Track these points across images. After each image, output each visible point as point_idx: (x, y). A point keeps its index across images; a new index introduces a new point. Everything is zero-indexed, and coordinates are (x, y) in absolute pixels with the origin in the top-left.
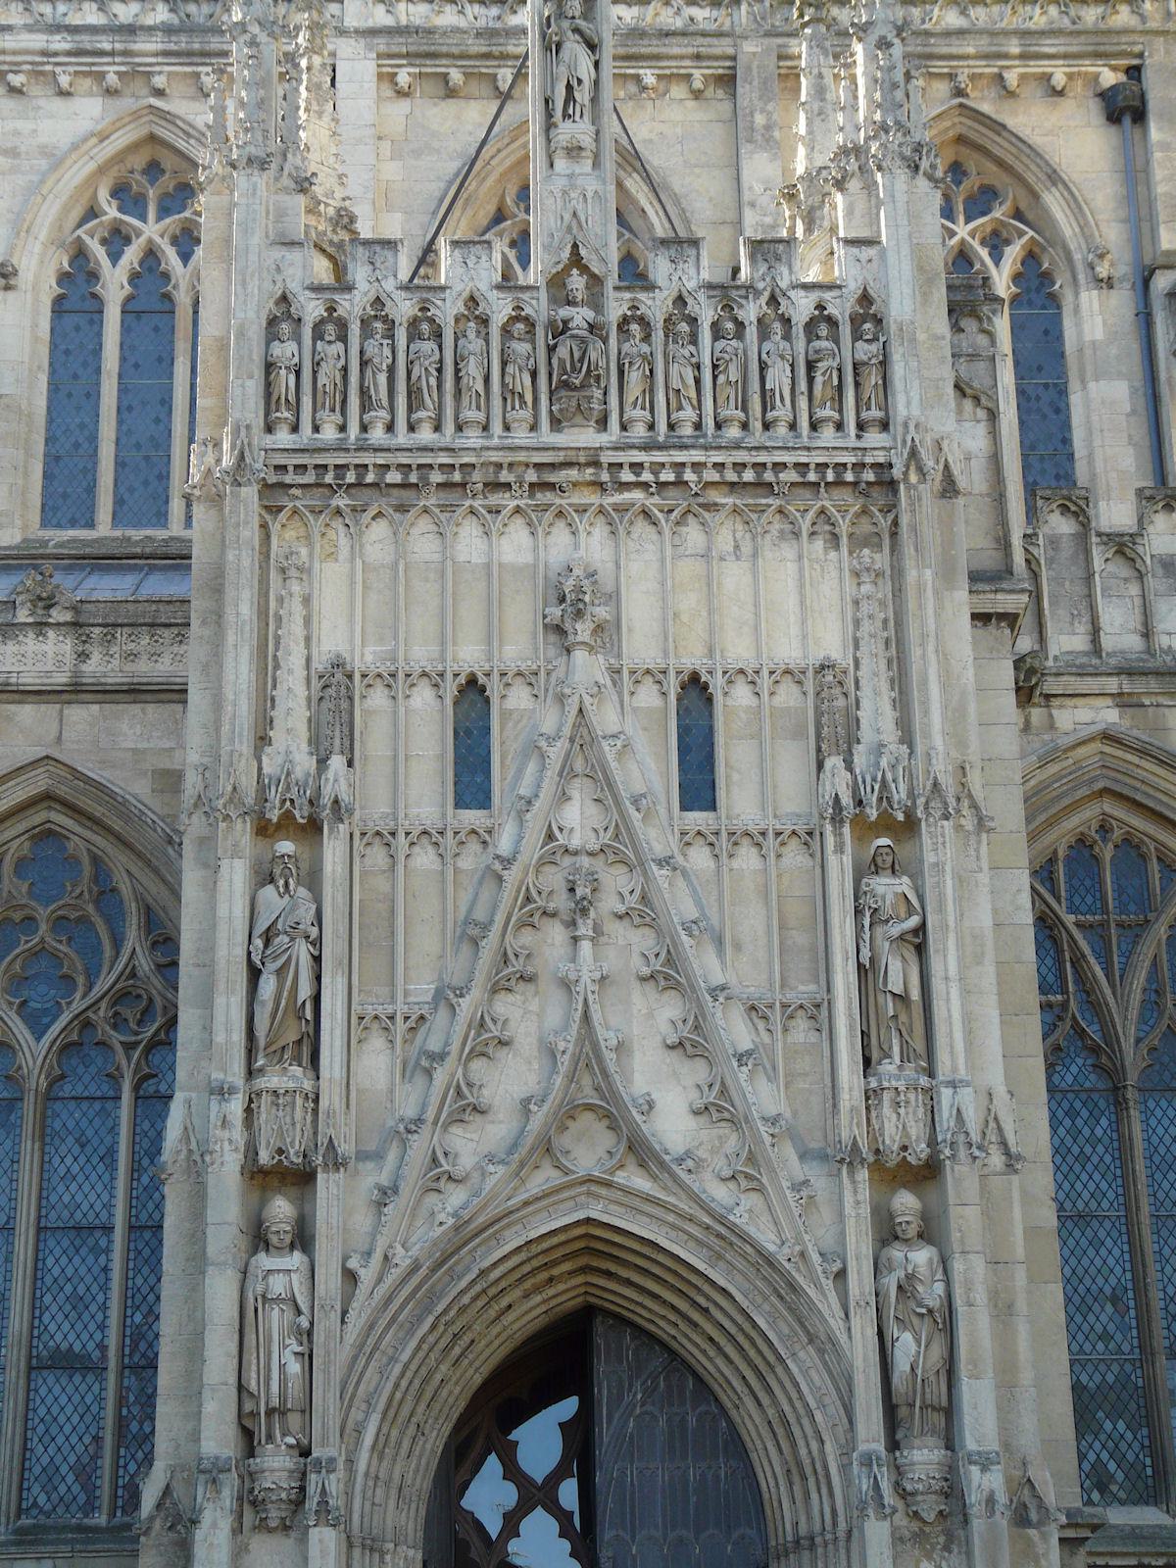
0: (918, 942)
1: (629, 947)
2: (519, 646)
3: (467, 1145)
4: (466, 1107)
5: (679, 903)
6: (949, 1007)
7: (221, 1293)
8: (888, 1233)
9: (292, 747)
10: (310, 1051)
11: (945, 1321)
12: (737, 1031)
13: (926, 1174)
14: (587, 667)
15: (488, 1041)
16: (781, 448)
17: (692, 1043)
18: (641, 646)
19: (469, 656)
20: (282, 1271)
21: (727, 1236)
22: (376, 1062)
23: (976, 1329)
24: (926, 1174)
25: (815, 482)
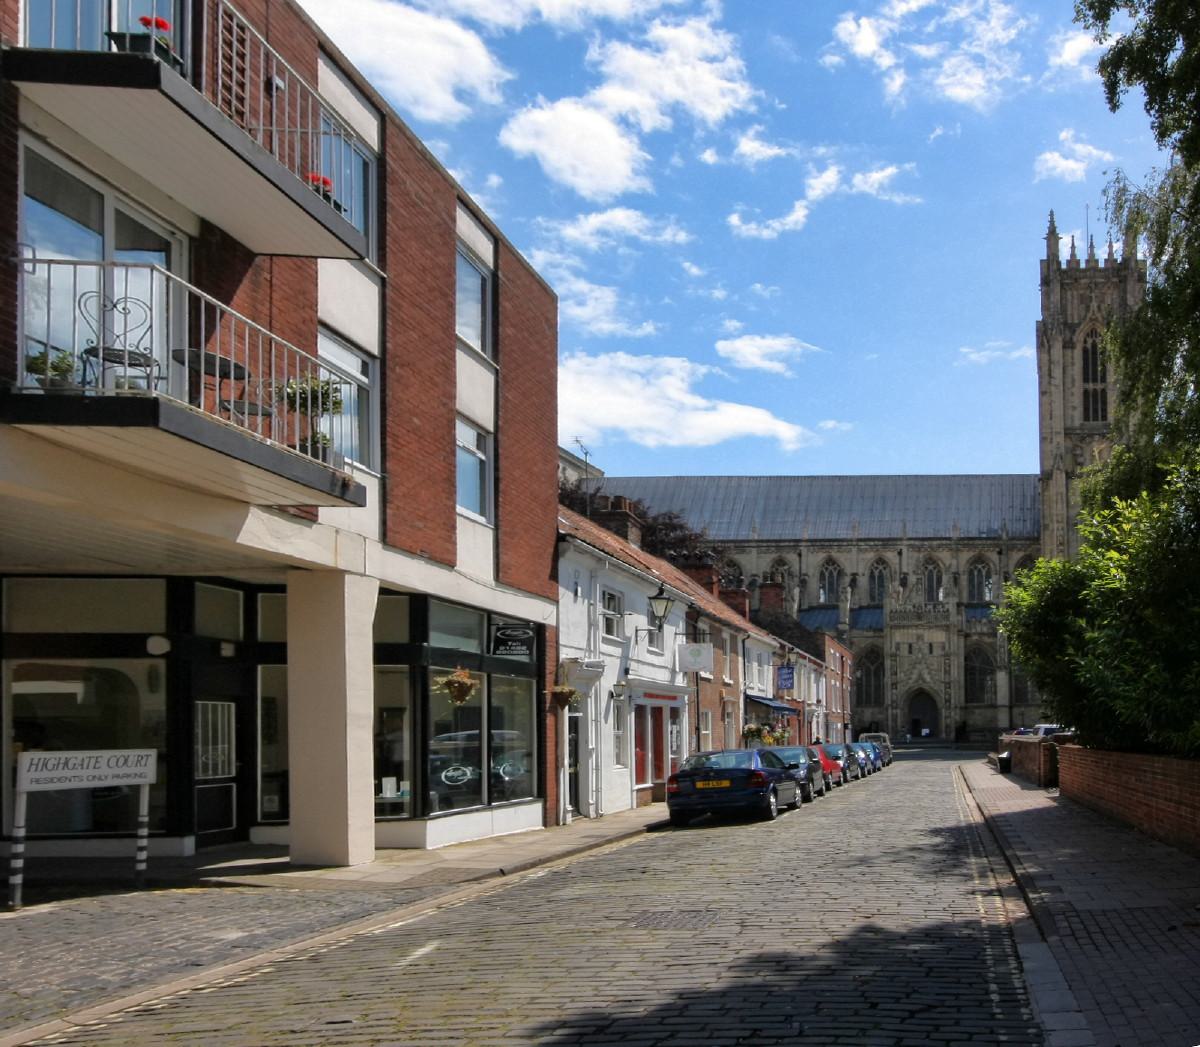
0: (950, 666)
1: (924, 666)
2: (915, 641)
3: (911, 681)
4: (910, 679)
5: (928, 662)
6: (952, 672)
7: (889, 694)
8: (946, 688)
9: (894, 649)
10: (896, 674)
11: (950, 695)
12: (933, 672)
13: (949, 683)
14: (920, 643)
15: (911, 673)
16: (939, 624)
17: (929, 673)
18: (926, 640)
19: (910, 641)
20: (894, 691)
21: (931, 688)
22: (902, 675)
23: (952, 695)
24: (949, 683)
25: (941, 626)
